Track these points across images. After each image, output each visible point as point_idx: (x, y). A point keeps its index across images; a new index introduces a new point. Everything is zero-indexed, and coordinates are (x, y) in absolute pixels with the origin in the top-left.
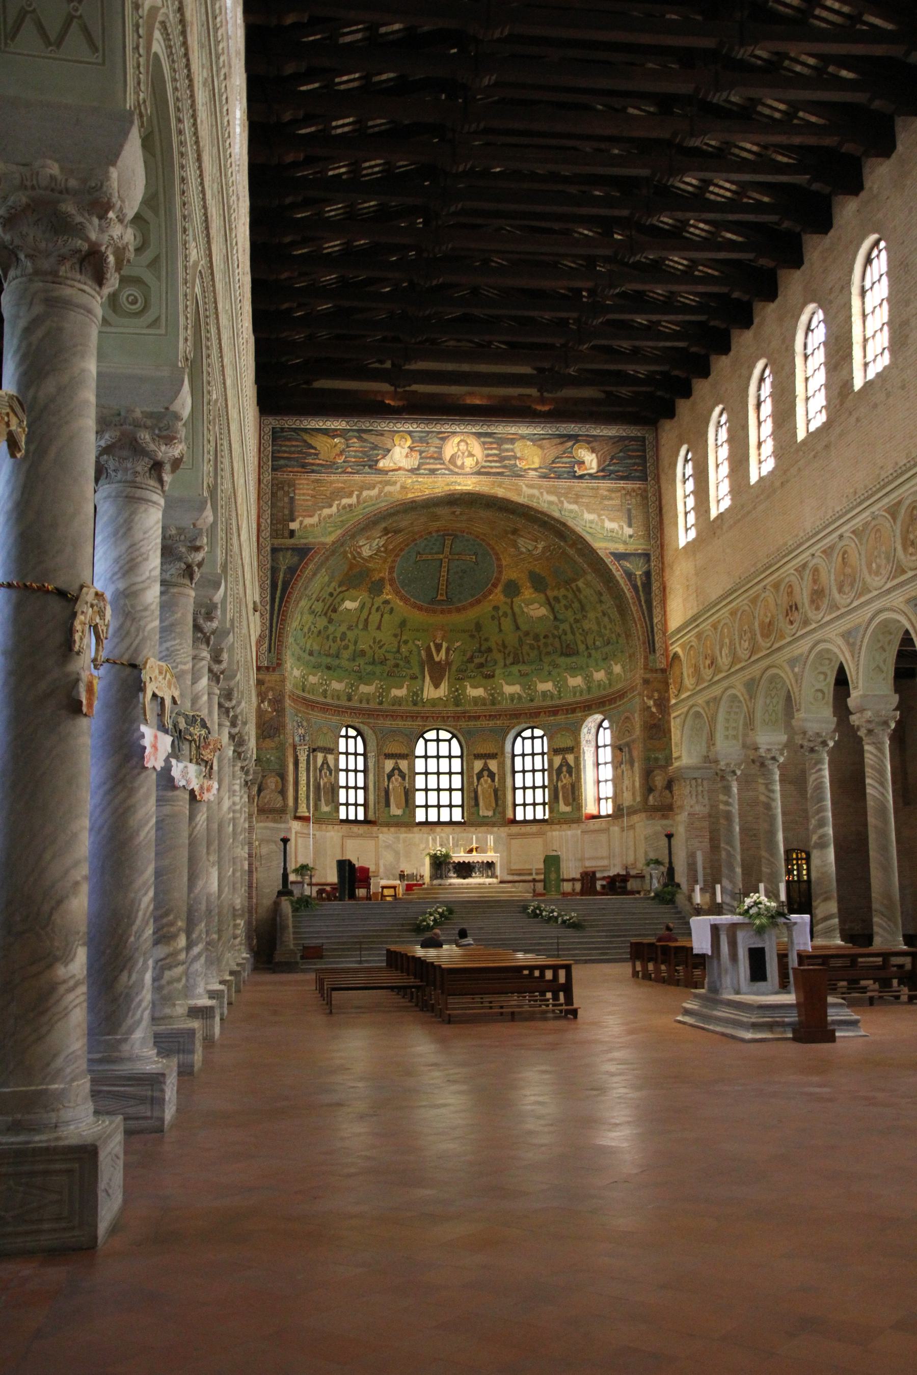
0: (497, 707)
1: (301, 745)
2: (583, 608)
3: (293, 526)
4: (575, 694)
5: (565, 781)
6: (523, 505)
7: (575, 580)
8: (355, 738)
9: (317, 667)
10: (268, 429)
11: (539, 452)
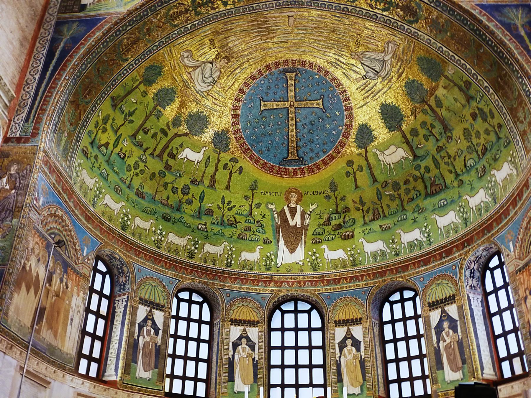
0: (359, 267)
1: (120, 296)
2: (446, 128)
4: (448, 233)
5: (448, 340)
7: (433, 90)
8: (201, 304)
9: (148, 213)
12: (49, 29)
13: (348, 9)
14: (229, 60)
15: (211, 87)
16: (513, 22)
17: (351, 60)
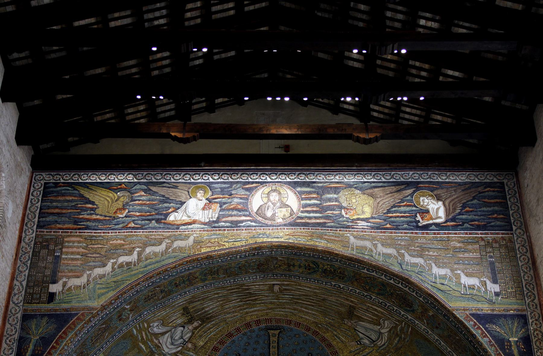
3: (54, 288)
6: (350, 259)
10: (39, 186)
11: (371, 201)
12: (16, 324)
13: (340, 286)
14: (203, 322)
15: (180, 348)
16: (507, 337)
17: (343, 325)
